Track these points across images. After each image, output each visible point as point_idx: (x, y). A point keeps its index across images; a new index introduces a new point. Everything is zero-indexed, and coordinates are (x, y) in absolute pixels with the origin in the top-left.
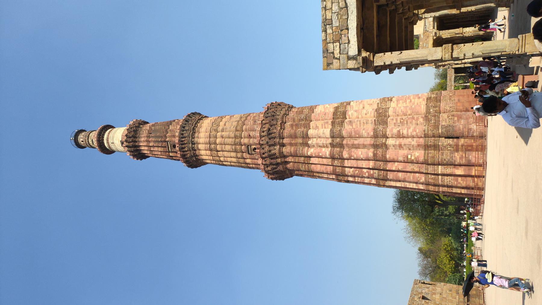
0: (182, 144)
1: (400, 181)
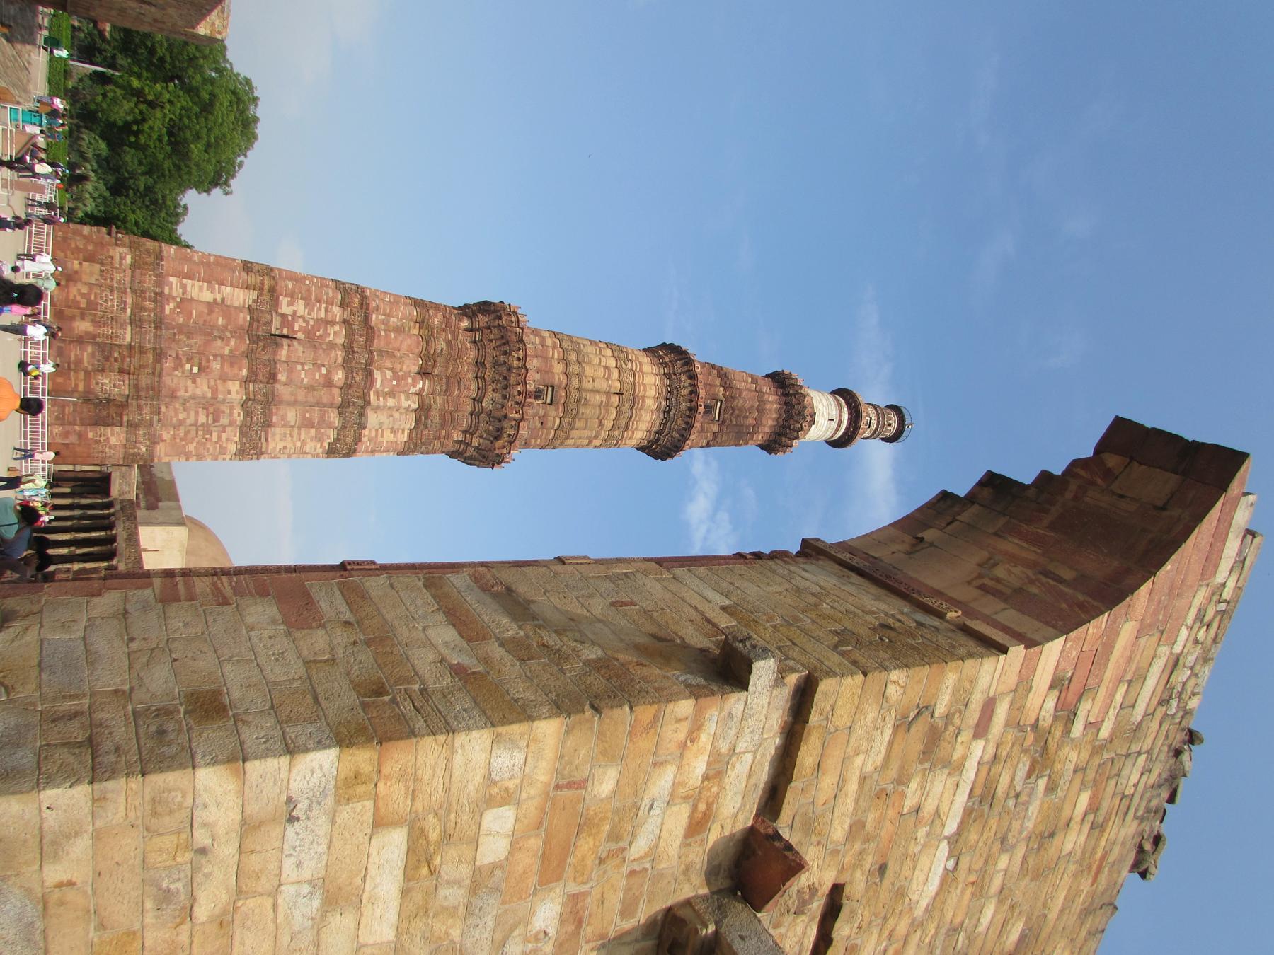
1: (223, 299)
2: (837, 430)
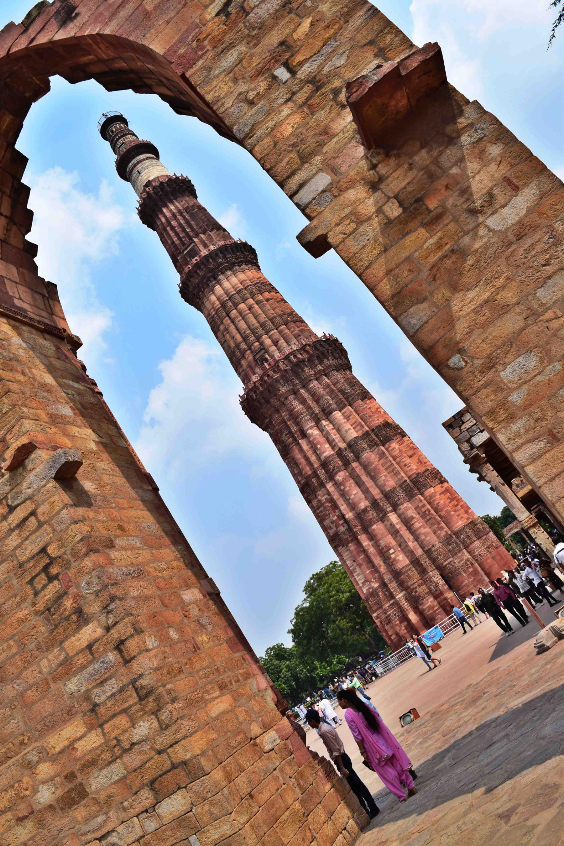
0: (203, 264)
1: (354, 561)
2: (140, 161)
